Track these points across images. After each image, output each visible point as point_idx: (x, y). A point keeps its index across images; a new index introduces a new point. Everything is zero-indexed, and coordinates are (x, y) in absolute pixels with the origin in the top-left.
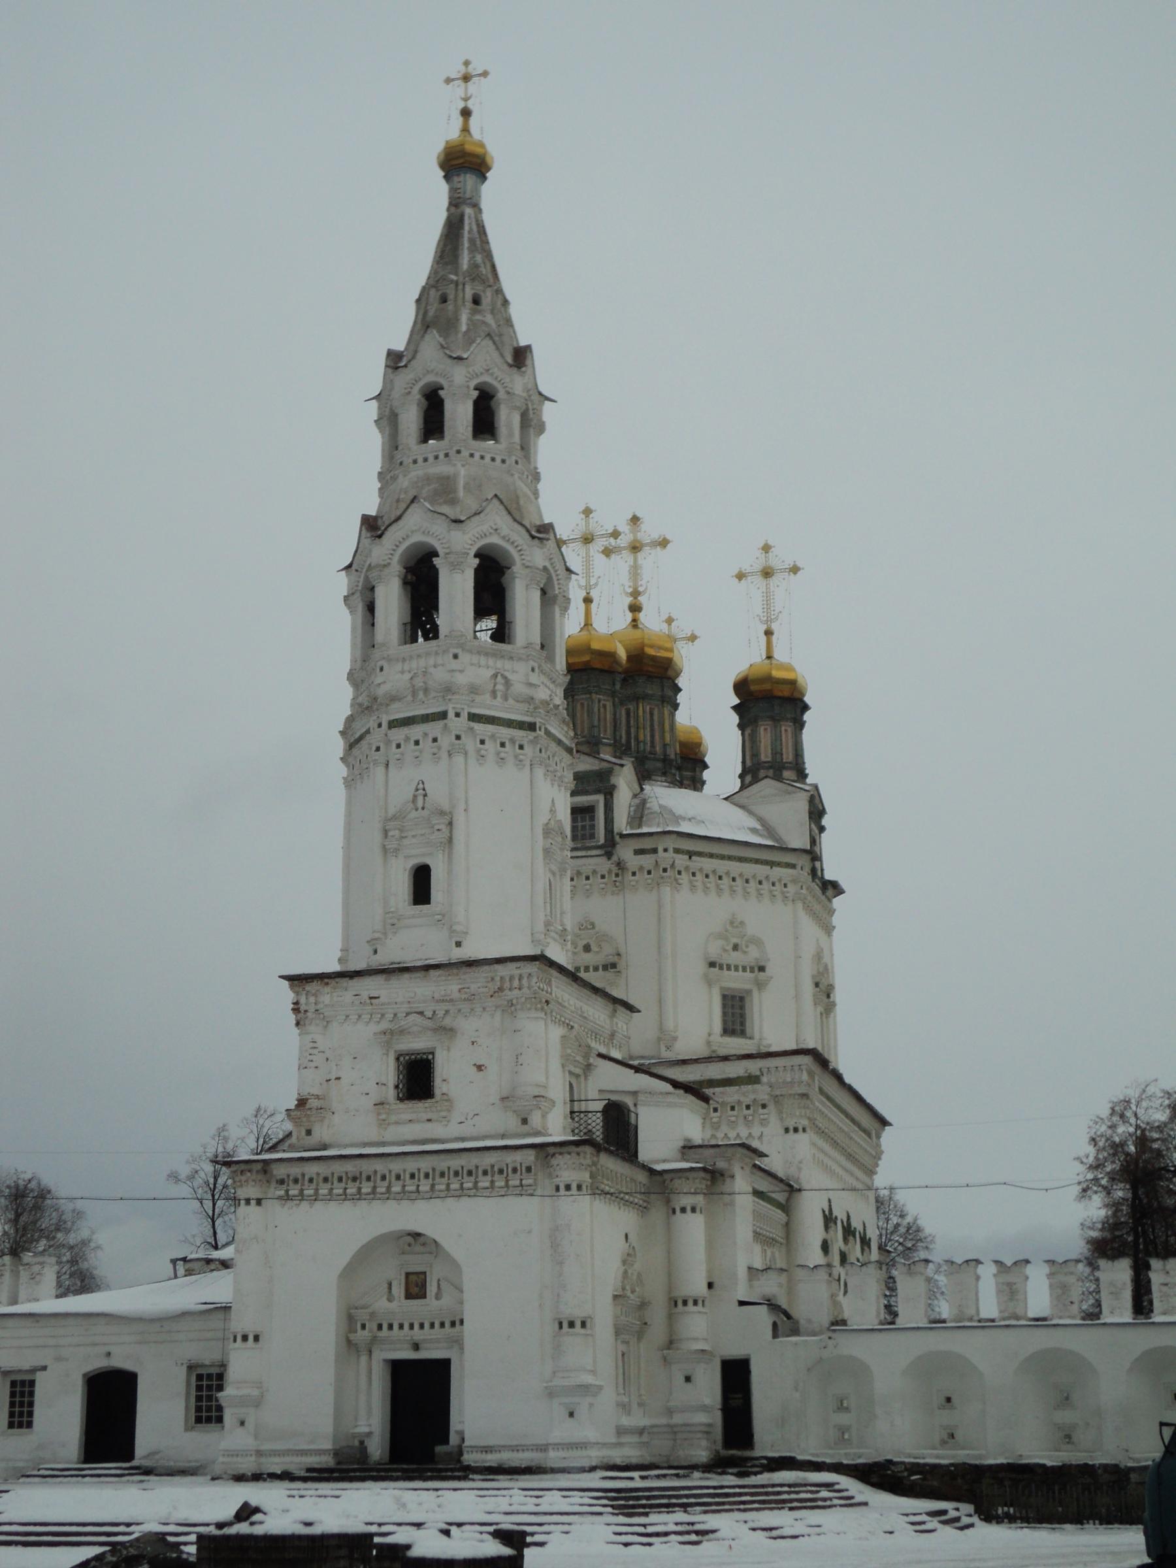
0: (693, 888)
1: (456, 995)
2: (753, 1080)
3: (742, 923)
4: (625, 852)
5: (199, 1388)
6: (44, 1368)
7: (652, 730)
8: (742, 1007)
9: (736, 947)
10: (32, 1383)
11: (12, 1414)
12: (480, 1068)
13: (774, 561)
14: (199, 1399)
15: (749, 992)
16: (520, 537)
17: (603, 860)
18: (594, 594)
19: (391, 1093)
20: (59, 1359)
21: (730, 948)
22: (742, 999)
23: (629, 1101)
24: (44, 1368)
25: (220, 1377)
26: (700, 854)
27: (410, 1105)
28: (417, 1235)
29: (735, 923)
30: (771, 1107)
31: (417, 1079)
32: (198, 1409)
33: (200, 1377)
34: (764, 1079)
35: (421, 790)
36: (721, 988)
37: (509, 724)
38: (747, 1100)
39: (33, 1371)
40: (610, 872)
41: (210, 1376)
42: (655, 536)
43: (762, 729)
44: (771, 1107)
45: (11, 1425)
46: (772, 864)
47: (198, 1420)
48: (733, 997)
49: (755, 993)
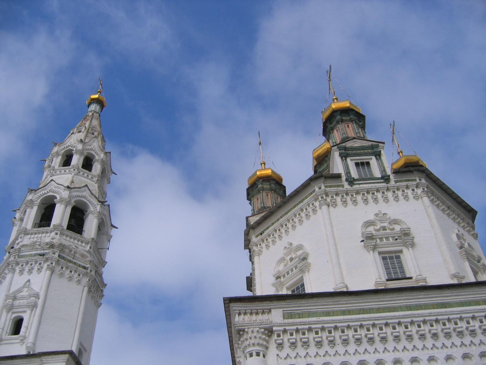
8: (400, 263)
15: (401, 251)
22: (398, 257)
36: (380, 253)
48: (391, 258)
49: (405, 250)
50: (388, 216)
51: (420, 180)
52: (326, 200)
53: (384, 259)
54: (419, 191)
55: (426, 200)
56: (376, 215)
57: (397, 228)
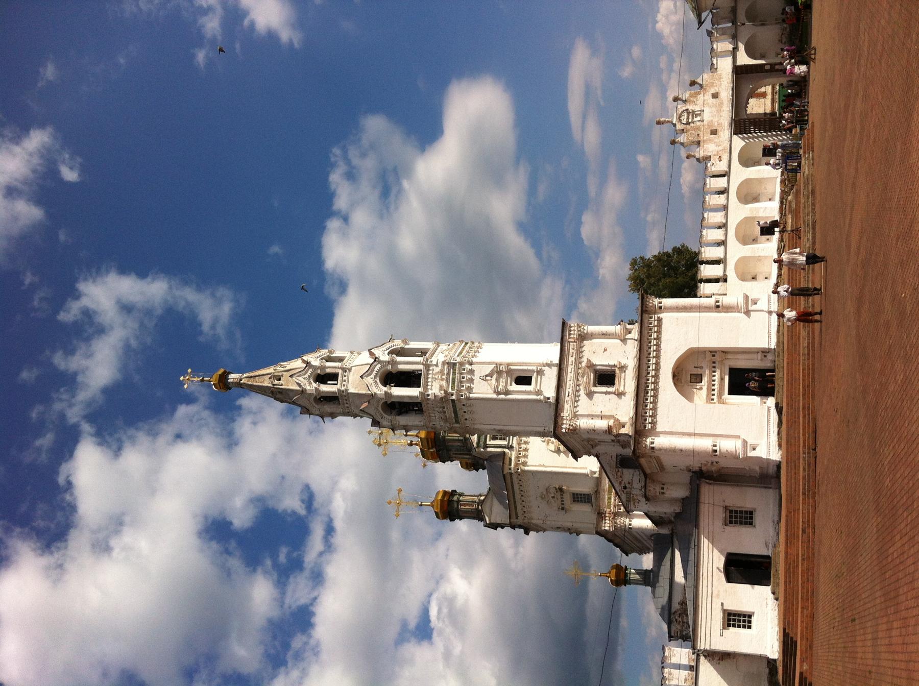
1: (573, 359)
5: (736, 523)
6: (722, 604)
10: (729, 614)
11: (744, 627)
12: (605, 350)
14: (741, 523)
16: (390, 344)
19: (611, 389)
20: (718, 595)
24: (722, 604)
25: (731, 511)
27: (616, 382)
28: (674, 376)
31: (606, 378)
32: (746, 523)
33: (731, 522)
35: (484, 378)
37: (463, 349)
39: (724, 611)
41: (731, 517)
45: (750, 627)
47: (751, 524)
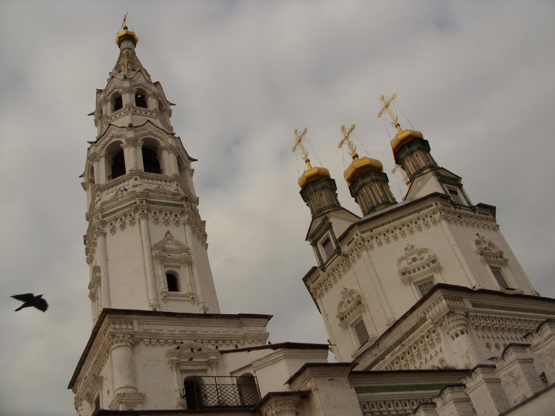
0: (380, 244)
2: (423, 320)
3: (412, 246)
4: (345, 249)
7: (374, 196)
9: (414, 260)
13: (386, 99)
17: (339, 257)
18: (308, 158)
21: (410, 261)
23: (250, 371)
26: (377, 227)
29: (410, 249)
30: (439, 330)
34: (427, 317)
36: (415, 284)
38: (424, 333)
40: (343, 260)
42: (350, 127)
43: (406, 162)
44: (439, 330)
46: (418, 211)
50: (415, 248)
51: (437, 205)
52: (364, 245)
53: (420, 287)
54: (437, 216)
55: (444, 222)
56: (406, 249)
57: (426, 256)
